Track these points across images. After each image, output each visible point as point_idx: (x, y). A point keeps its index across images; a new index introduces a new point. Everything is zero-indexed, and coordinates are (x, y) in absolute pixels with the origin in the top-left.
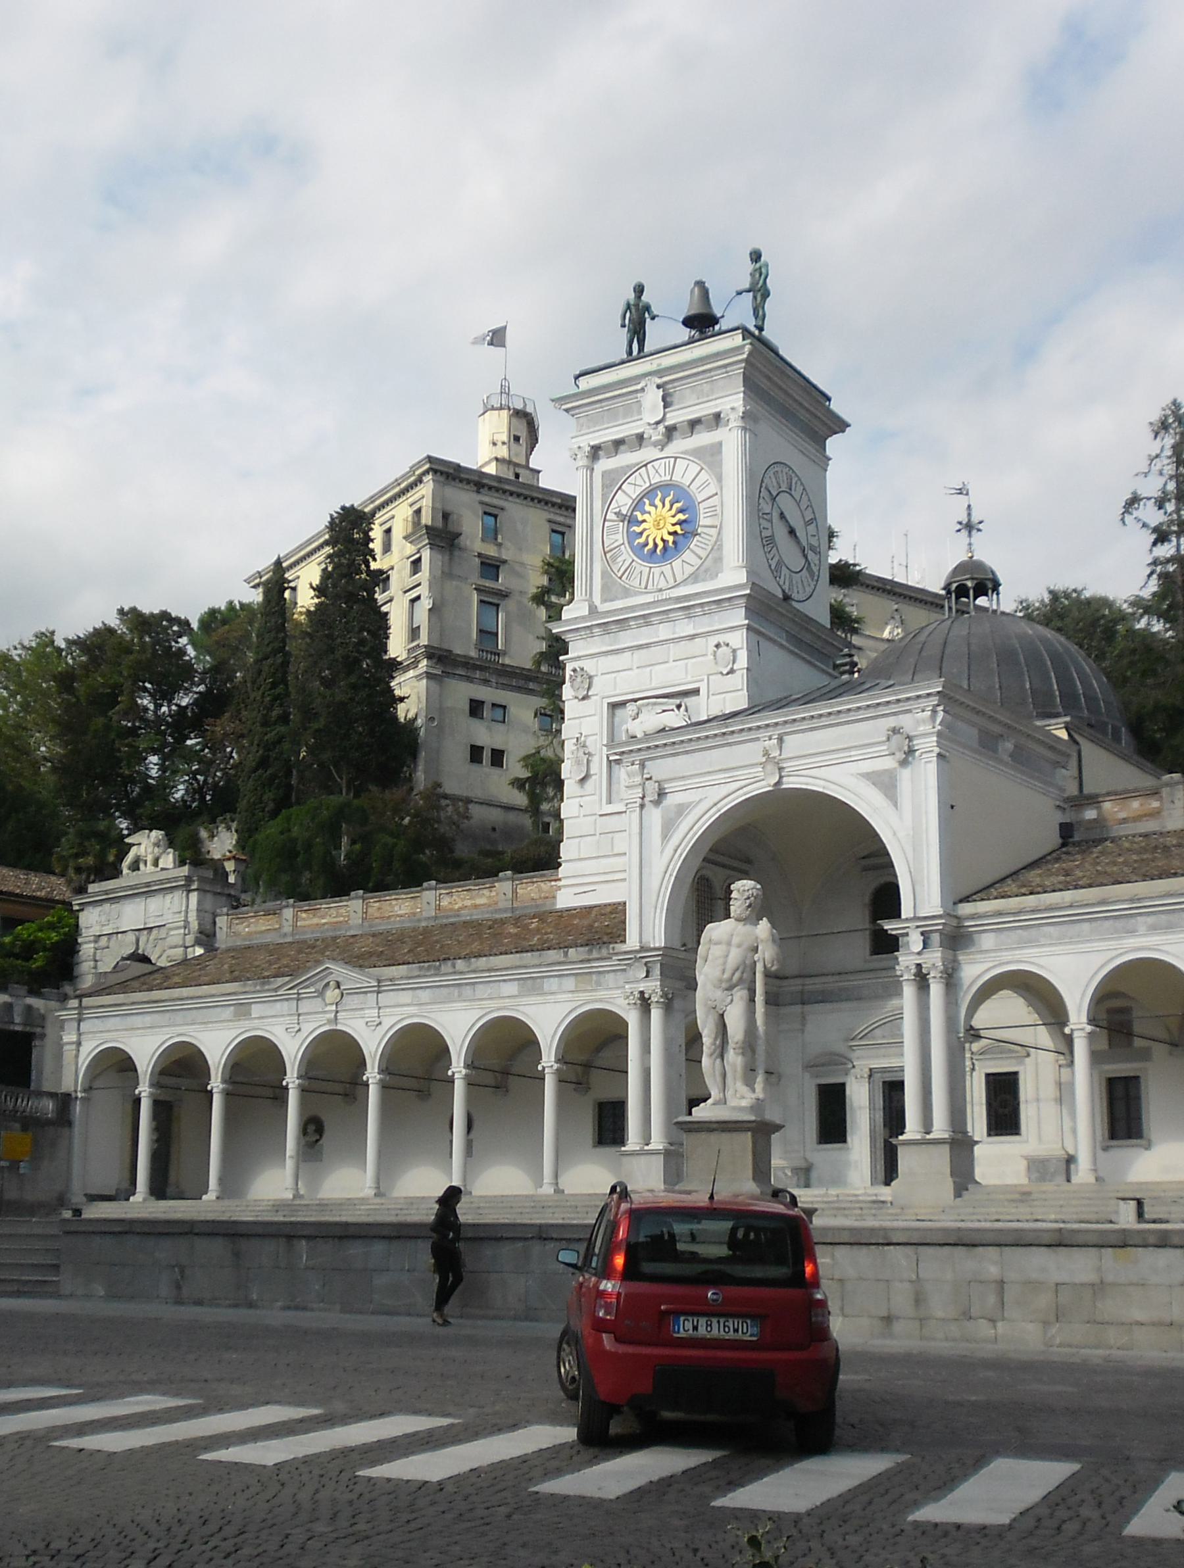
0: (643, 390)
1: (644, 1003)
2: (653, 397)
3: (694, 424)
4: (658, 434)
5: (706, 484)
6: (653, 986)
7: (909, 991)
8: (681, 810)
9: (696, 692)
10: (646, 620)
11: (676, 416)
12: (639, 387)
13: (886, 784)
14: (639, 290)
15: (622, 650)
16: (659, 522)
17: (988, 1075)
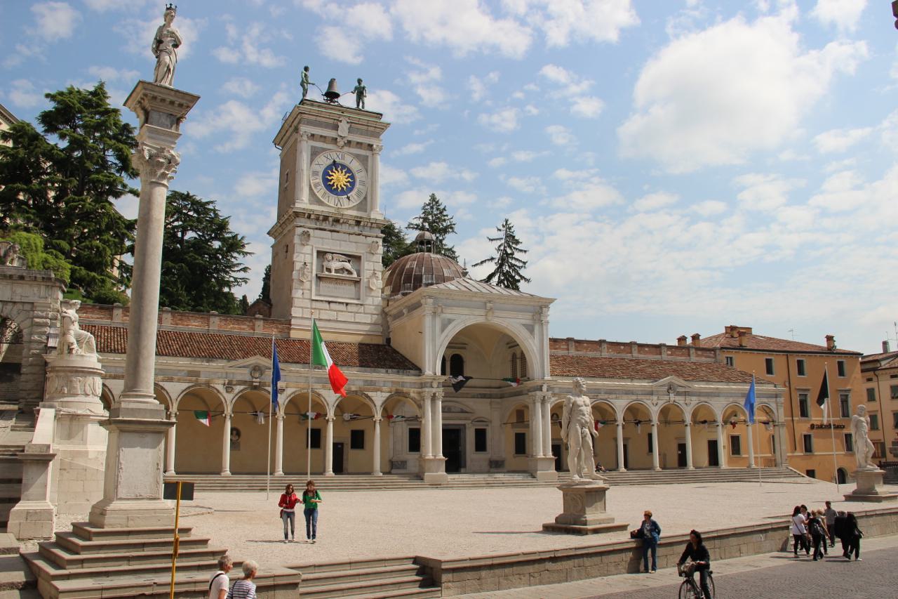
0: (341, 121)
1: (434, 398)
2: (344, 127)
3: (359, 145)
4: (341, 143)
5: (359, 171)
6: (440, 392)
7: (539, 405)
8: (450, 321)
9: (358, 258)
10: (337, 221)
11: (351, 138)
12: (340, 119)
13: (531, 329)
14: (306, 69)
15: (325, 230)
16: (339, 178)
17: (476, 429)
